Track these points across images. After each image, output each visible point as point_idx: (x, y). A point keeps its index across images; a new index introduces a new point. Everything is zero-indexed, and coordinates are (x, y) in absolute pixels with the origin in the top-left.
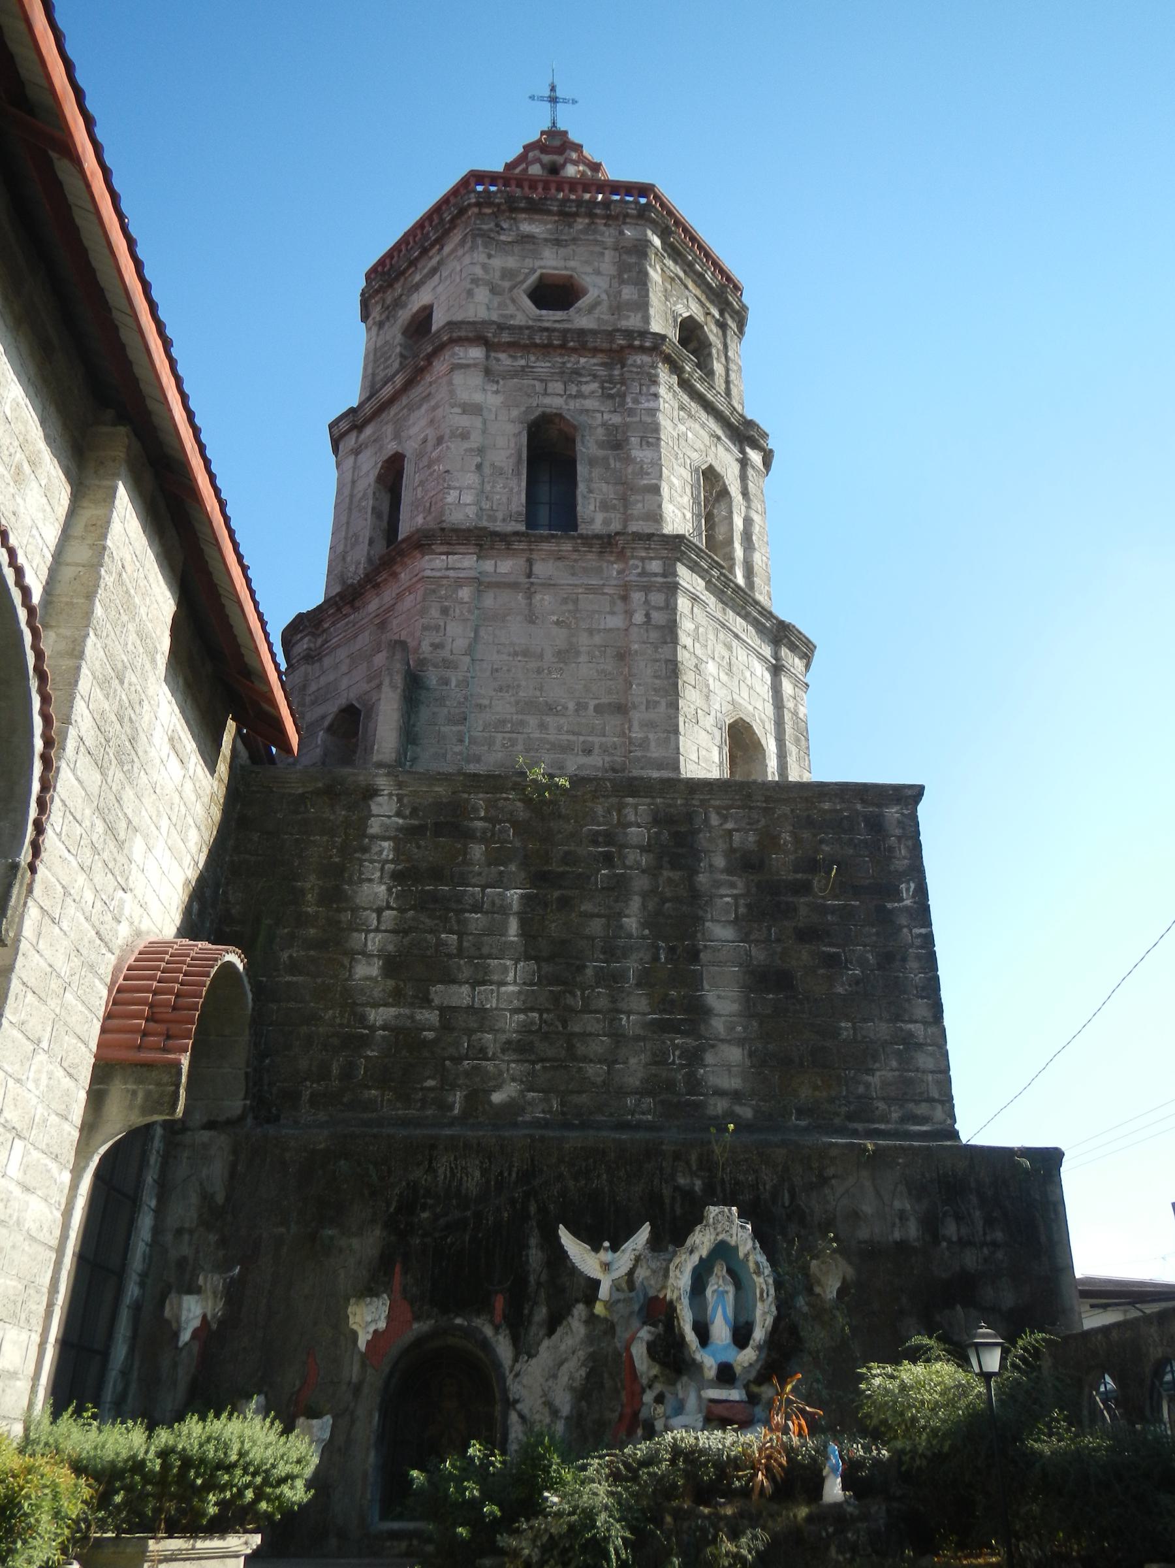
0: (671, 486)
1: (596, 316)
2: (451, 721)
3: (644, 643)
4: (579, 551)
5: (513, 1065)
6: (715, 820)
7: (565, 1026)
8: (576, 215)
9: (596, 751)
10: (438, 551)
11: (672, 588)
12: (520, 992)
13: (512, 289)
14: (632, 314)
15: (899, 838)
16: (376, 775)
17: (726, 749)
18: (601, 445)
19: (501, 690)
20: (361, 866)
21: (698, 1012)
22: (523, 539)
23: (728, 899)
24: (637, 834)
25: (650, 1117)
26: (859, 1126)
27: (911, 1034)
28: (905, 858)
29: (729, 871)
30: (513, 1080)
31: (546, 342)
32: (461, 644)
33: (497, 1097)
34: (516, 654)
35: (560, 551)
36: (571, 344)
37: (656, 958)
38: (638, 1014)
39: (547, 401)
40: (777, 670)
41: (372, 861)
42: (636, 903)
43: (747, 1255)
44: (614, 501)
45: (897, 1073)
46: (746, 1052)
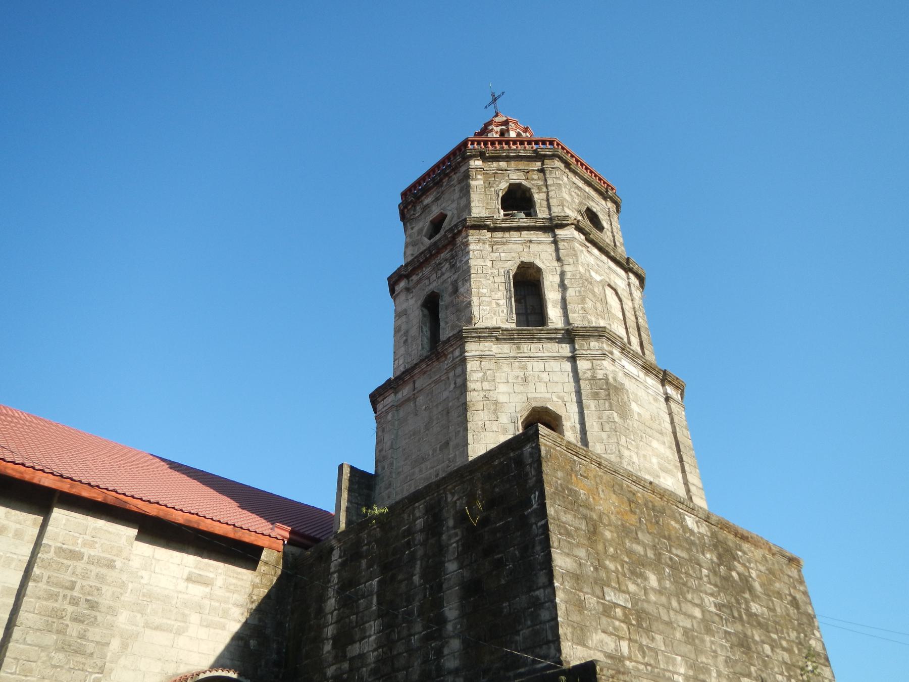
2: (387, 488)
4: (429, 365)
7: (391, 652)
8: (441, 180)
10: (380, 400)
11: (464, 361)
12: (376, 639)
14: (464, 213)
15: (530, 465)
20: (328, 591)
21: (441, 621)
22: (407, 373)
23: (454, 545)
24: (420, 523)
27: (537, 598)
34: (411, 436)
35: (422, 369)
37: (425, 596)
38: (418, 633)
40: (573, 359)
45: (531, 629)
46: (461, 641)
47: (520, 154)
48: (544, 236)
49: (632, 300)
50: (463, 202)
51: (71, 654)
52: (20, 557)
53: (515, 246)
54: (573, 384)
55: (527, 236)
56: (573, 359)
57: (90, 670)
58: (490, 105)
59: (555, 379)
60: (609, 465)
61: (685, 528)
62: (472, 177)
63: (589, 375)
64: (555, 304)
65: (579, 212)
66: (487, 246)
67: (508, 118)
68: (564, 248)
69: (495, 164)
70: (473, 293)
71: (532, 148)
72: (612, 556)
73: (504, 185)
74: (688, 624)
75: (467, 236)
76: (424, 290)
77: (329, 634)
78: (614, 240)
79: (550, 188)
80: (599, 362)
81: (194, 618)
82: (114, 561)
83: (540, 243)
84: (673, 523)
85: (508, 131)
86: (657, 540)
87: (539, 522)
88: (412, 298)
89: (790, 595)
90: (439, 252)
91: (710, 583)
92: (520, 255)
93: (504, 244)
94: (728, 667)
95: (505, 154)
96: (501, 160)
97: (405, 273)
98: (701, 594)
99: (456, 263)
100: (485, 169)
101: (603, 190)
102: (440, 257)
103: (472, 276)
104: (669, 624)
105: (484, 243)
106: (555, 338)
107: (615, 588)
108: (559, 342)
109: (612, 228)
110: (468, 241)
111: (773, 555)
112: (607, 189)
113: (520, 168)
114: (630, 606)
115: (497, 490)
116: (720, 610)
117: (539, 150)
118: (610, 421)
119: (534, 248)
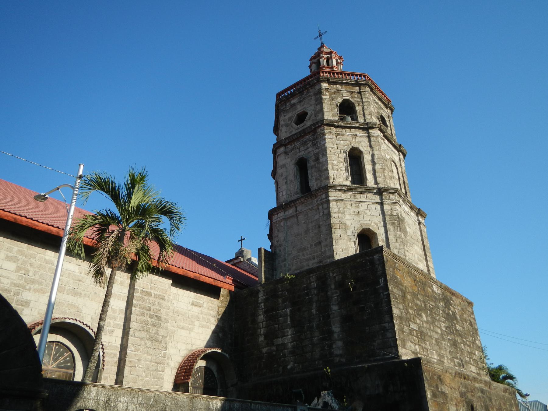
0: (333, 165)
1: (311, 119)
2: (283, 261)
3: (323, 221)
5: (291, 358)
6: (331, 275)
8: (303, 91)
9: (316, 257)
10: (275, 214)
11: (328, 201)
12: (291, 337)
13: (291, 123)
14: (319, 114)
15: (379, 265)
16: (258, 287)
17: (357, 241)
18: (314, 161)
19: (293, 248)
20: (258, 311)
21: (331, 333)
23: (336, 297)
24: (314, 284)
25: (321, 366)
26: (372, 359)
27: (385, 327)
28: (381, 270)
29: (335, 289)
30: (292, 362)
31: (296, 137)
32: (282, 238)
33: (289, 367)
34: (296, 236)
36: (302, 135)
37: (320, 320)
39: (300, 154)
40: (382, 204)
41: (260, 310)
42: (314, 305)
43: (331, 404)
44: (319, 177)
47: (348, 82)
48: (363, 133)
49: (401, 168)
50: (318, 108)
51: (153, 341)
52: (124, 295)
53: (348, 137)
54: (382, 217)
55: (354, 132)
56: (382, 204)
57: (162, 349)
58: (317, 37)
59: (373, 214)
60: (407, 263)
61: (433, 291)
62: (323, 93)
63: (389, 213)
64: (370, 171)
65: (378, 117)
66: (334, 136)
67: (332, 50)
68: (373, 140)
69: (334, 86)
70: (329, 163)
71: (354, 78)
72: (411, 307)
73: (340, 100)
74: (436, 336)
75: (323, 130)
76: (296, 155)
77: (261, 333)
78: (392, 132)
79: (365, 104)
80: (394, 206)
81: (196, 323)
82: (164, 296)
83: (361, 136)
84: (429, 289)
85: (331, 58)
86: (424, 298)
87: (384, 292)
88: (289, 158)
89: (469, 320)
90: (306, 134)
91: (443, 317)
92: (351, 143)
93: (342, 135)
94: (450, 355)
95: (340, 81)
96: (337, 84)
97: (284, 143)
98: (440, 322)
99: (317, 143)
100: (330, 89)
101: (387, 103)
102: (306, 138)
103: (328, 153)
104: (431, 336)
105: (333, 135)
106: (372, 192)
107: (412, 322)
108: (374, 194)
109: (390, 125)
110: (324, 132)
111: (463, 301)
112: (388, 102)
113: (348, 90)
114: (418, 330)
115: (359, 274)
116: (446, 329)
117: (358, 80)
118: (400, 237)
119: (358, 139)
